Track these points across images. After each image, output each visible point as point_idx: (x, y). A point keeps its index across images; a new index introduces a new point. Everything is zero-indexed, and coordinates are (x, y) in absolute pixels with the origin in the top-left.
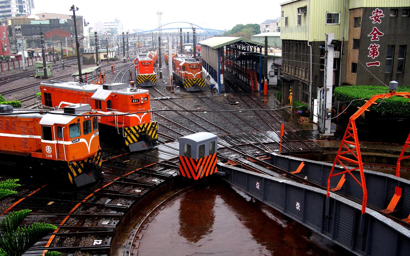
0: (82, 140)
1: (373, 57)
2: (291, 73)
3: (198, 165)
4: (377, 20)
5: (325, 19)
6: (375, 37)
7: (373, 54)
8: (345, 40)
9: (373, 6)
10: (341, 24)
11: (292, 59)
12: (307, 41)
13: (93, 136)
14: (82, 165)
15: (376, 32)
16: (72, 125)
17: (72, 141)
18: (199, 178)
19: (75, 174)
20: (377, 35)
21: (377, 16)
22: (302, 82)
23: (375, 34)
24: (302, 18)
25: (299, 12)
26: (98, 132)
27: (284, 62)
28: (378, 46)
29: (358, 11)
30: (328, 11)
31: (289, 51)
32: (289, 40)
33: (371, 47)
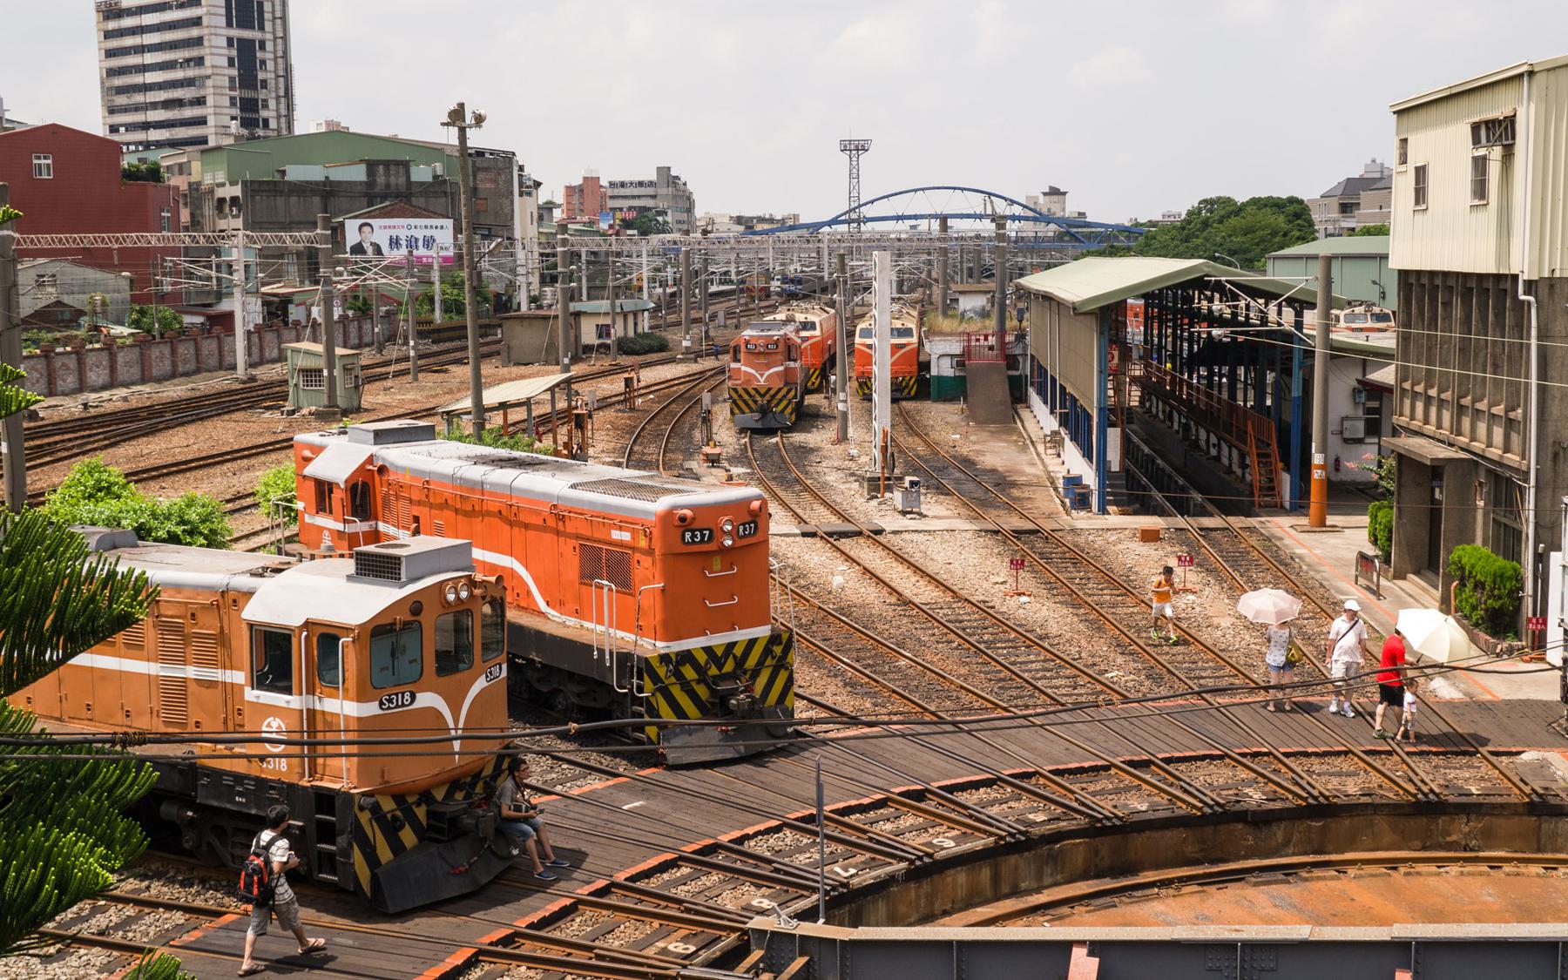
0: (426, 699)
2: (1439, 426)
11: (1444, 363)
12: (1515, 277)
13: (481, 684)
14: (421, 812)
16: (381, 631)
17: (381, 704)
19: (385, 854)
22: (1489, 471)
24: (1494, 169)
25: (1476, 141)
26: (504, 666)
27: (1403, 374)
31: (1433, 324)
32: (1432, 274)
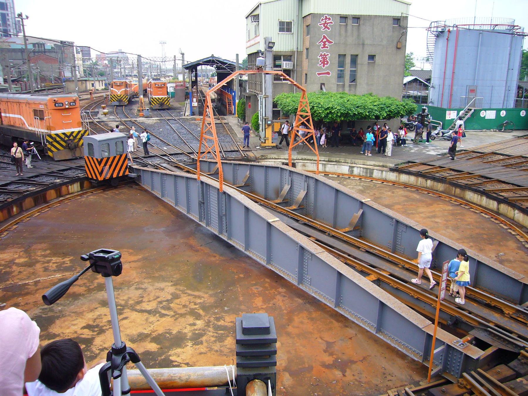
1: (324, 66)
3: (102, 165)
4: (326, 27)
5: (277, 28)
6: (324, 45)
7: (323, 63)
8: (299, 50)
9: (321, 13)
10: (295, 33)
15: (325, 40)
18: (104, 178)
20: (327, 43)
21: (325, 23)
23: (325, 42)
28: (328, 55)
29: (308, 17)
30: (280, 19)
33: (321, 55)
